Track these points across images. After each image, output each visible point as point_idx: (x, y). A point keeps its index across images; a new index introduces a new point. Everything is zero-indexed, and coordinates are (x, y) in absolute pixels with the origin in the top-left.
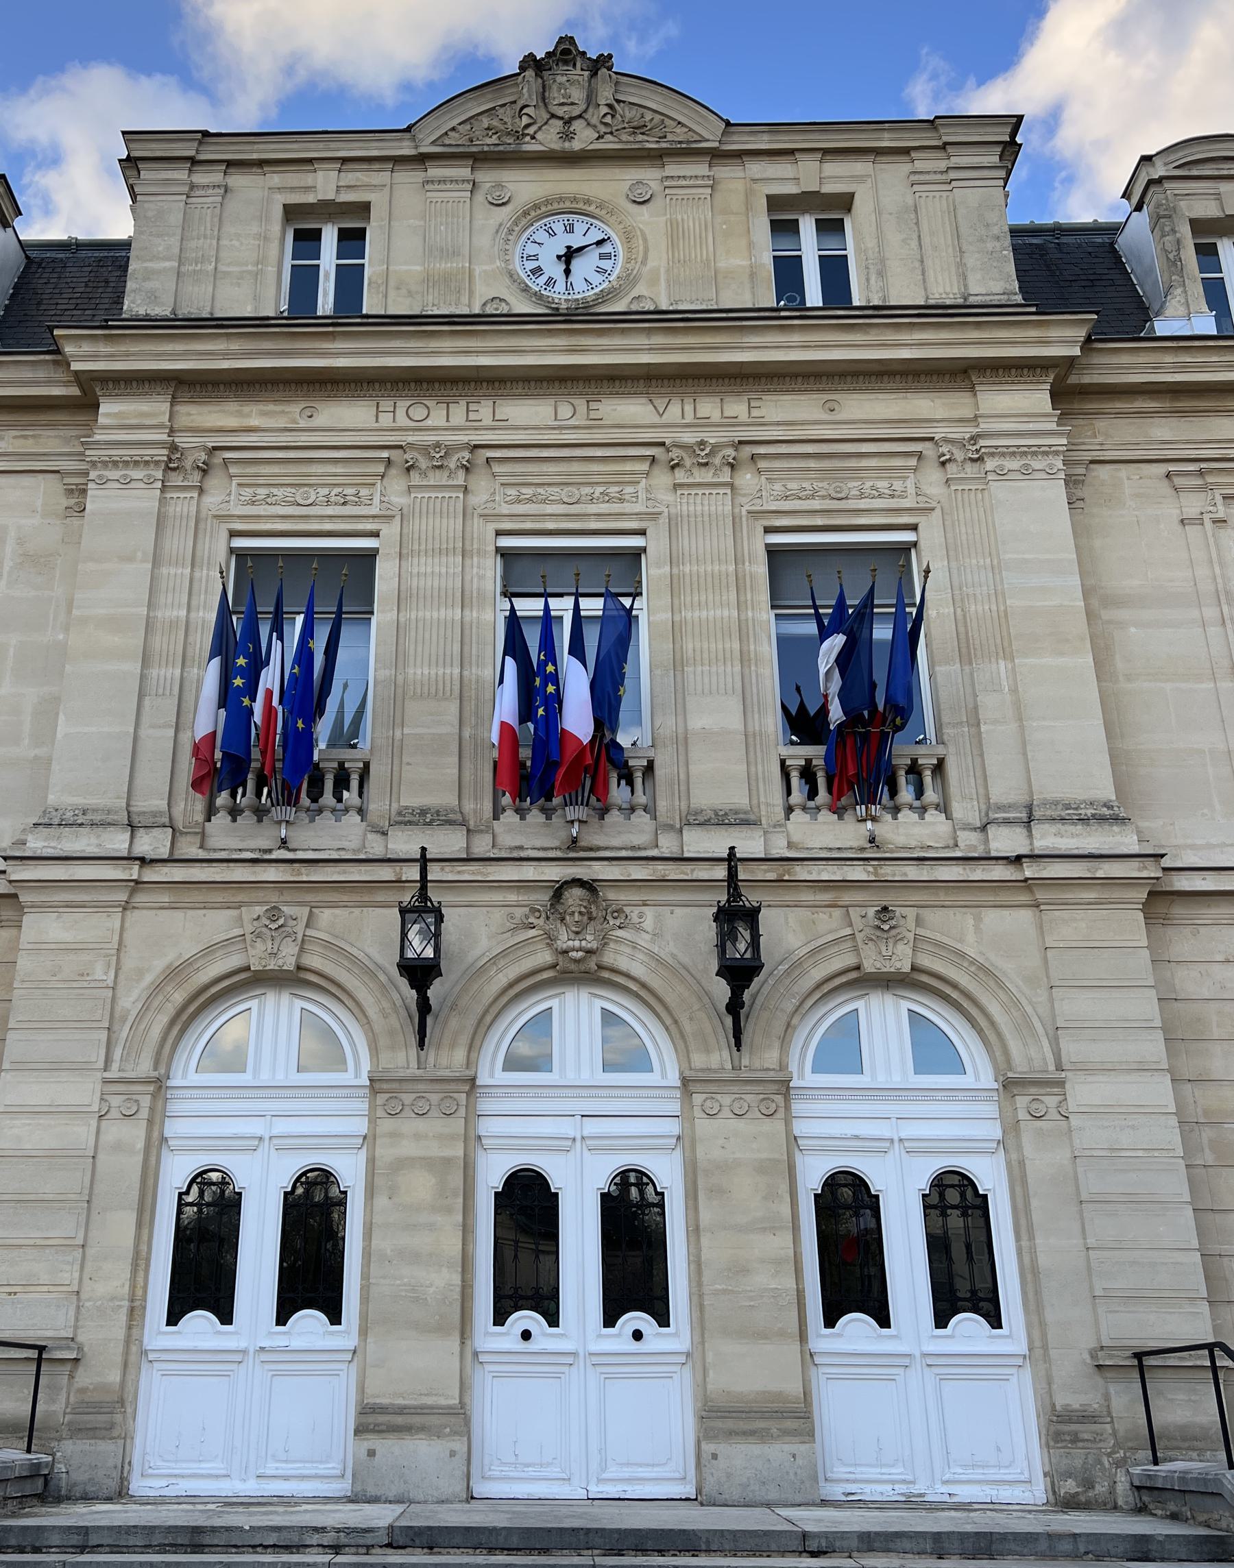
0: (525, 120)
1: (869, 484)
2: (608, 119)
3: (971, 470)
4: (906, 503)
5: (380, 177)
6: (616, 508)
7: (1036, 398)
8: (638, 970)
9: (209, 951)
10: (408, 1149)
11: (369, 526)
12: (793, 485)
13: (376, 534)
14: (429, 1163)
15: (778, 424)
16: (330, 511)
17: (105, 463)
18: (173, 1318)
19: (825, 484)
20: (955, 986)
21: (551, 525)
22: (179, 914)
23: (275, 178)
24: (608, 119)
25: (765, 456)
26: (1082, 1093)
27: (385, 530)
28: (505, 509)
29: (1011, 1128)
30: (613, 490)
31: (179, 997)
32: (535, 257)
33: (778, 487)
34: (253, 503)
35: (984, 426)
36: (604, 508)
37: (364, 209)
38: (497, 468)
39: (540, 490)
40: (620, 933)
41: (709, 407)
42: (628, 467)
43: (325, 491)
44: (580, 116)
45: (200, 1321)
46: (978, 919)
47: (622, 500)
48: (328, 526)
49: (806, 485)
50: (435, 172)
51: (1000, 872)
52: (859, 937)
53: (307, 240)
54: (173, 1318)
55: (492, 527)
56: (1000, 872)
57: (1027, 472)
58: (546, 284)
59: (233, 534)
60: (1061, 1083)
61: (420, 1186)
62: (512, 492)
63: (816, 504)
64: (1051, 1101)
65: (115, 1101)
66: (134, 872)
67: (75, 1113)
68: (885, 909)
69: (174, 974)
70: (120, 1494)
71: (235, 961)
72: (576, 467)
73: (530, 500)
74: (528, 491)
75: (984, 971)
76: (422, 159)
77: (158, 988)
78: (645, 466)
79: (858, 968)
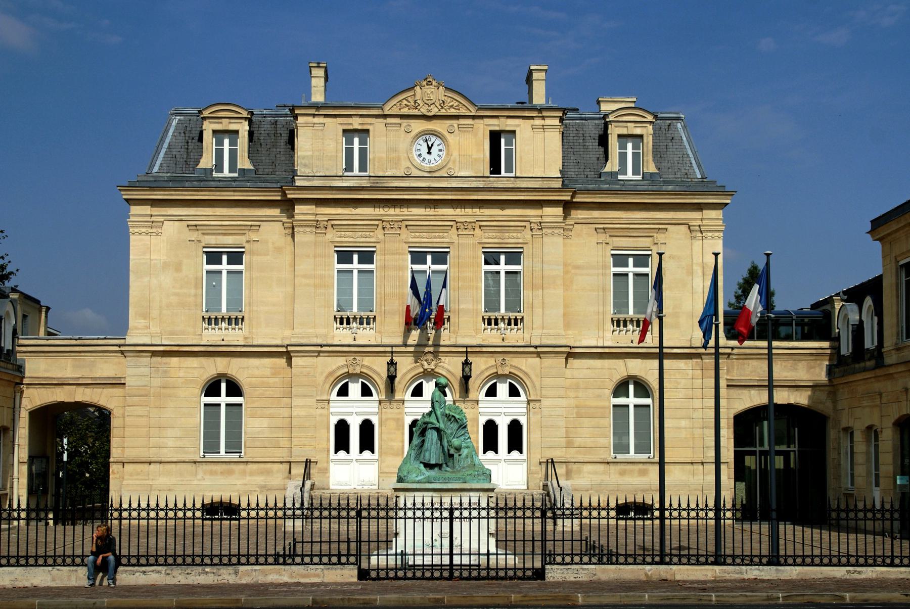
0: (417, 104)
1: (511, 234)
2: (442, 105)
3: (540, 233)
4: (520, 241)
5: (373, 120)
6: (441, 240)
7: (559, 211)
8: (444, 373)
9: (339, 368)
10: (390, 416)
11: (373, 245)
12: (490, 234)
13: (375, 247)
14: (394, 419)
15: (487, 216)
16: (362, 240)
17: (299, 226)
18: (336, 452)
19: (499, 234)
20: (519, 377)
21: (424, 245)
22: (330, 358)
23: (339, 120)
24: (442, 105)
25: (483, 226)
26: (545, 402)
27: (378, 245)
28: (411, 240)
29: (528, 411)
30: (441, 234)
31: (332, 379)
32: (419, 150)
33: (486, 234)
34: (340, 237)
35: (545, 219)
36: (438, 240)
37: (367, 131)
38: (408, 227)
39: (421, 234)
40: (440, 364)
41: (469, 211)
42: (445, 228)
43: (360, 233)
44: (434, 103)
45: (342, 453)
46: (526, 360)
47: (443, 238)
48: (361, 245)
49: (494, 234)
50: (389, 120)
51: (532, 350)
52: (498, 365)
53: (350, 142)
54: (336, 452)
55: (407, 245)
56: (532, 350)
57: (553, 234)
58: (423, 160)
59: (335, 246)
60: (540, 401)
61: (392, 424)
62: (413, 234)
63: (496, 241)
64: (538, 405)
65: (319, 404)
66: (319, 349)
67: (310, 407)
68: (504, 359)
69: (331, 374)
70: (328, 489)
71: (346, 370)
72: (430, 228)
73: (418, 237)
74: (417, 234)
75: (526, 374)
76: (385, 116)
77: (327, 377)
78: (450, 228)
79: (497, 372)
